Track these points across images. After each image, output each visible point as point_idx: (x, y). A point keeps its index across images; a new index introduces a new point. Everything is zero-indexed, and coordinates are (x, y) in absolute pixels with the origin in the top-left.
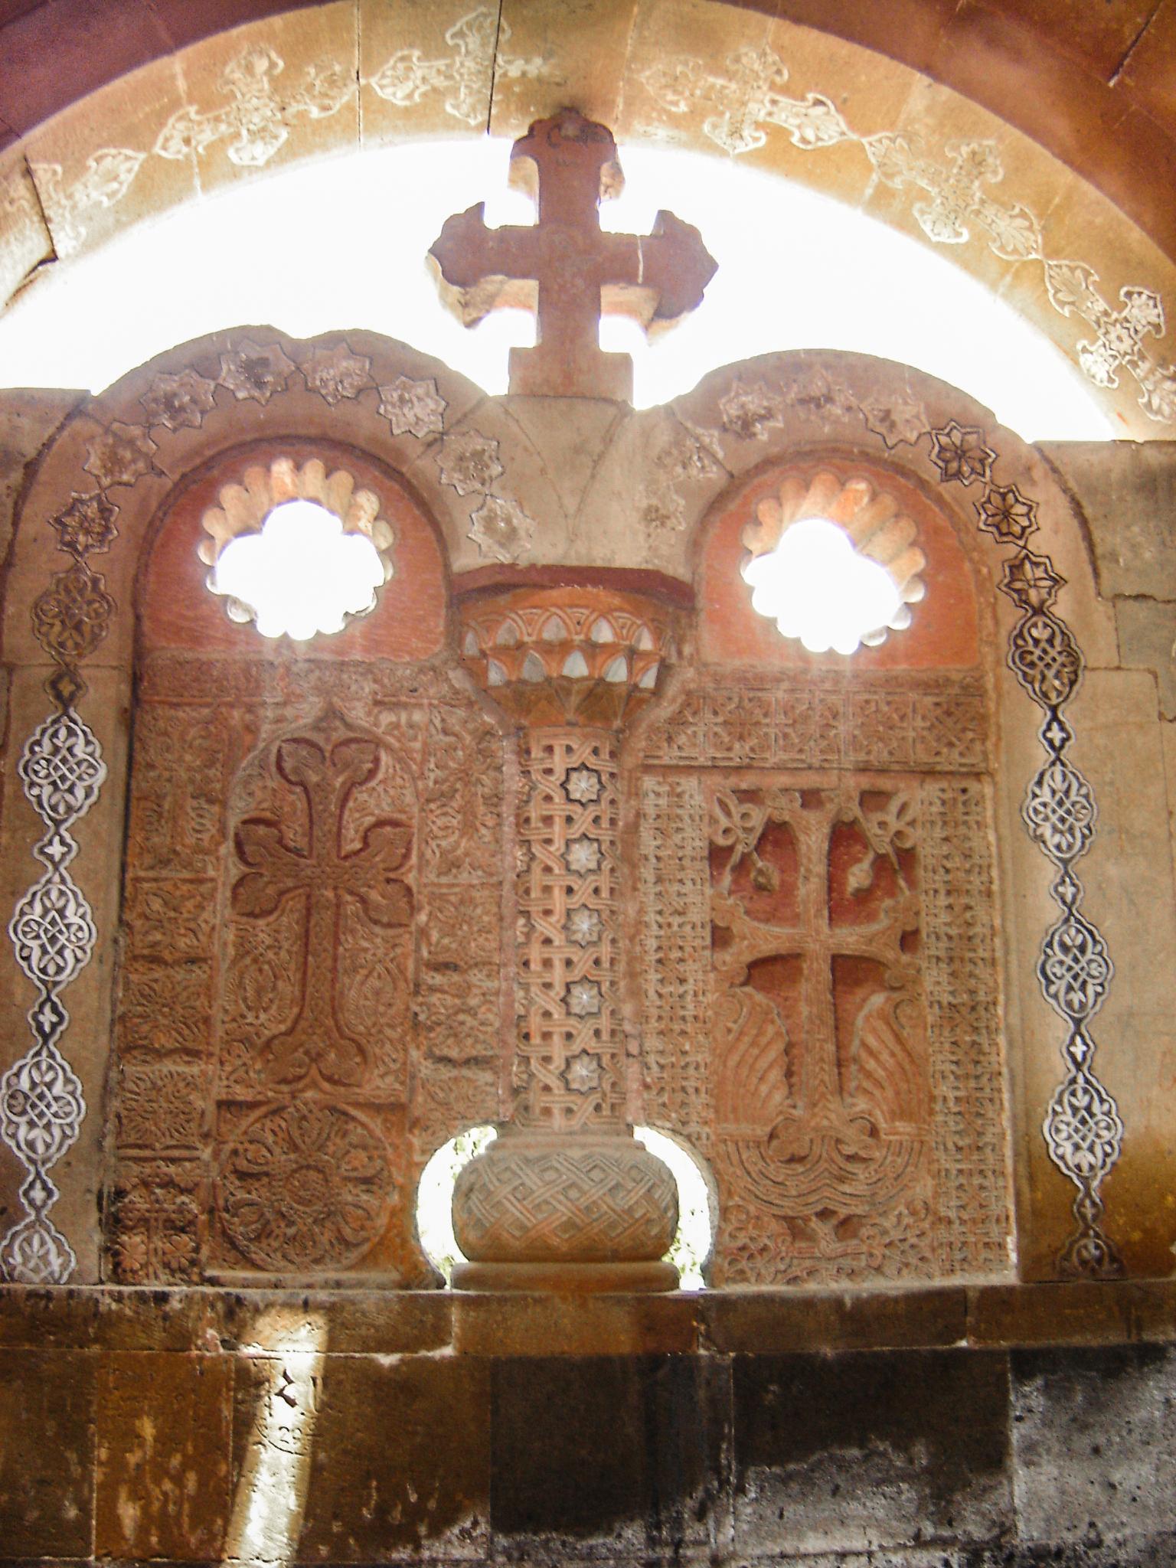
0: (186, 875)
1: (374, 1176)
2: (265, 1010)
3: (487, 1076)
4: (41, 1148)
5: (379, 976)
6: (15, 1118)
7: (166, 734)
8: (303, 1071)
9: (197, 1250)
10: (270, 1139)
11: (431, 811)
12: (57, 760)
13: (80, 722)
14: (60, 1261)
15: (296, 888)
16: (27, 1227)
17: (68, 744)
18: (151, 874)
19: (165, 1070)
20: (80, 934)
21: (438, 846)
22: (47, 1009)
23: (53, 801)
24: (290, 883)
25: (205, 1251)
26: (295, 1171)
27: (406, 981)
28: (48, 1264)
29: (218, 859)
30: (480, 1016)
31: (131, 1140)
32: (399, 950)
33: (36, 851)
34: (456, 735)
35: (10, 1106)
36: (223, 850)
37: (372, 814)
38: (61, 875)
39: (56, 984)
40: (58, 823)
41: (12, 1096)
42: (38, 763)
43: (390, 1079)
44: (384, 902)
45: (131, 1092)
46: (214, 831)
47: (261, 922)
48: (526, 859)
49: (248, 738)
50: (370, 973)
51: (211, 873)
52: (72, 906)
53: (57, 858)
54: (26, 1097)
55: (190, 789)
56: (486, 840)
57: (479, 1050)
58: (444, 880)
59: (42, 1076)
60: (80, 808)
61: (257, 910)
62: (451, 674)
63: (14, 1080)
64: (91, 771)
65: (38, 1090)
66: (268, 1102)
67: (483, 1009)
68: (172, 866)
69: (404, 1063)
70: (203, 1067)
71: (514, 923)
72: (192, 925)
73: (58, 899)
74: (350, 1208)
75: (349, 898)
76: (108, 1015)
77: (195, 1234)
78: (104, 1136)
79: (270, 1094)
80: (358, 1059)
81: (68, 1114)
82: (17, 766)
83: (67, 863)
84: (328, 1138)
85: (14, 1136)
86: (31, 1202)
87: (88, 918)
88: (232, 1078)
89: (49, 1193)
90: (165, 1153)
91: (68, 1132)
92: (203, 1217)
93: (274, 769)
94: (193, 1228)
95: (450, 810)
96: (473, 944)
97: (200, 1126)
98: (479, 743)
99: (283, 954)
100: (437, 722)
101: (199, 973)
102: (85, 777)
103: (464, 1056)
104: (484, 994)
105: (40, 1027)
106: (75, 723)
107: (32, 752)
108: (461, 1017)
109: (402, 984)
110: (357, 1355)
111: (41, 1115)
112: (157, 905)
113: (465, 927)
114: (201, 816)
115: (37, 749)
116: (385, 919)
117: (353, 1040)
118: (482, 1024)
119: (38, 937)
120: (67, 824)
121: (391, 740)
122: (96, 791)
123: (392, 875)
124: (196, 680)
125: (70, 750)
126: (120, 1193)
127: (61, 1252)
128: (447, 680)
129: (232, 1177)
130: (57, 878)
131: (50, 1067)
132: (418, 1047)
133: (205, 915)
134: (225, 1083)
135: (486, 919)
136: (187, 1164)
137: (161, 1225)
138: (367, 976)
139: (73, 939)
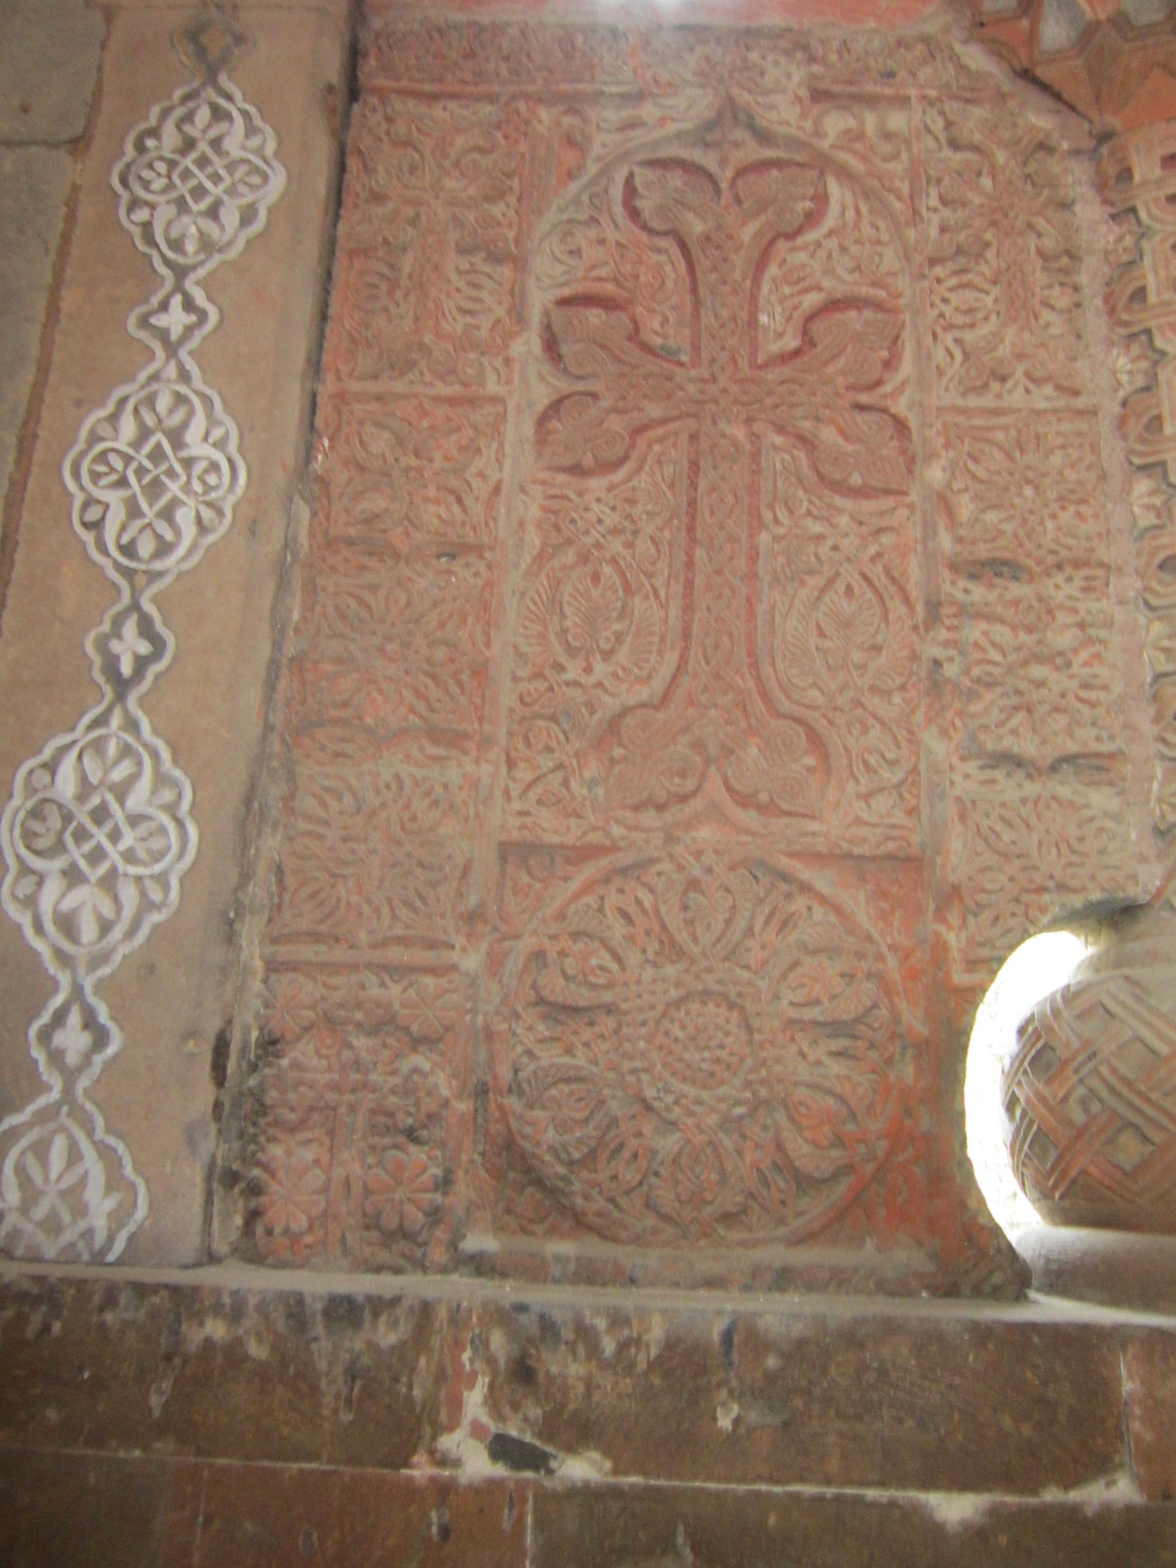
0: (441, 389)
1: (857, 1020)
2: (607, 655)
3: (1100, 799)
4: (88, 931)
5: (849, 590)
6: (36, 863)
7: (408, 144)
8: (690, 784)
9: (445, 1183)
10: (618, 931)
11: (939, 281)
12: (188, 162)
13: (238, 96)
14: (110, 1204)
15: (664, 421)
16: (44, 1116)
17: (212, 133)
18: (371, 387)
19: (386, 775)
20: (212, 479)
21: (958, 341)
22: (130, 628)
23: (174, 233)
24: (654, 411)
25: (463, 1191)
26: (677, 1004)
27: (906, 600)
28: (80, 1210)
29: (507, 361)
30: (1075, 669)
31: (303, 924)
32: (886, 539)
33: (132, 321)
34: (975, 148)
35: (29, 836)
36: (517, 348)
37: (819, 289)
38: (181, 367)
39: (154, 576)
40: (181, 272)
41: (36, 814)
42: (150, 166)
43: (882, 803)
44: (850, 448)
45: (307, 817)
46: (500, 311)
47: (597, 484)
48: (1144, 365)
49: (570, 158)
50: (830, 582)
51: (493, 387)
52: (199, 424)
53: (174, 336)
54: (67, 818)
55: (453, 236)
56: (1054, 331)
57: (1086, 739)
58: (973, 401)
59: (106, 772)
60: (230, 243)
61: (588, 460)
62: (958, 48)
63: (44, 777)
64: (255, 180)
65: (95, 801)
66: (614, 848)
67: (1084, 655)
68: (413, 375)
69: (915, 770)
70: (470, 768)
71: (1127, 489)
72: (454, 482)
73: (171, 411)
74: (801, 1093)
75: (778, 440)
76: (264, 651)
77: (443, 1144)
78: (241, 909)
79: (617, 831)
80: (810, 761)
81: (158, 856)
82: (109, 169)
83: (194, 343)
84: (749, 932)
85: (30, 902)
86: (56, 1057)
87: (233, 446)
88: (532, 795)
89: (101, 1039)
90: (377, 956)
91: (156, 895)
92: (462, 1107)
93: (619, 210)
94: (438, 1133)
95: (978, 281)
96: (1050, 525)
97: (460, 894)
98: (1025, 164)
99: (644, 546)
100: (938, 125)
101: (464, 574)
102: (242, 189)
103: (1051, 752)
104: (1082, 626)
105: (111, 666)
106: (229, 97)
107: (140, 148)
108: (1038, 671)
109: (897, 607)
110: (871, 1494)
111: (97, 856)
112: (380, 443)
113: (1028, 492)
114: (475, 286)
115: (150, 143)
116: (856, 480)
117: (799, 721)
118: (1085, 686)
119: (123, 482)
120: (201, 272)
121: (844, 157)
122: (262, 215)
123: (864, 398)
124: (470, 55)
125: (216, 144)
126: (271, 1045)
127: (114, 1181)
128: (954, 58)
129: (529, 1016)
130: (171, 371)
131: (126, 751)
132: (945, 733)
133: (478, 464)
134: (517, 805)
135: (1070, 474)
136: (429, 981)
137: (361, 1121)
138: (823, 591)
139: (197, 487)
